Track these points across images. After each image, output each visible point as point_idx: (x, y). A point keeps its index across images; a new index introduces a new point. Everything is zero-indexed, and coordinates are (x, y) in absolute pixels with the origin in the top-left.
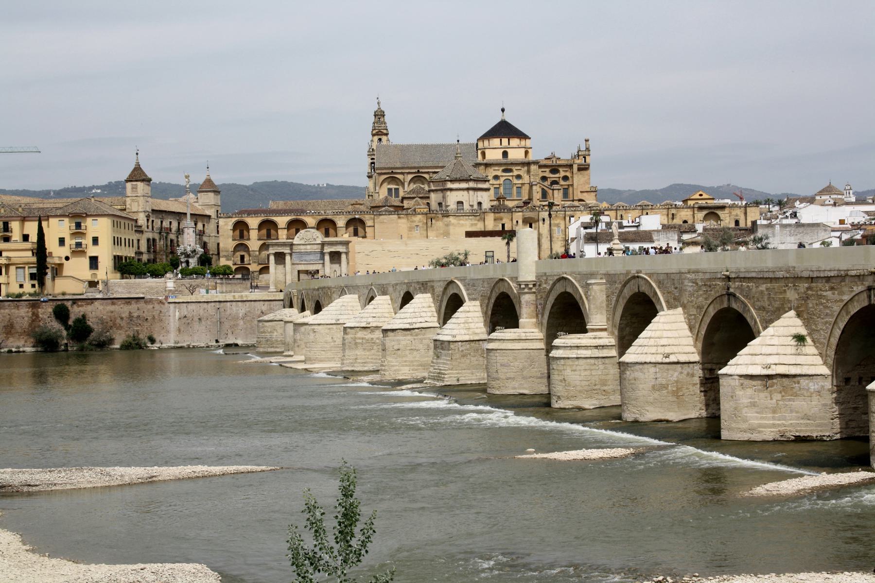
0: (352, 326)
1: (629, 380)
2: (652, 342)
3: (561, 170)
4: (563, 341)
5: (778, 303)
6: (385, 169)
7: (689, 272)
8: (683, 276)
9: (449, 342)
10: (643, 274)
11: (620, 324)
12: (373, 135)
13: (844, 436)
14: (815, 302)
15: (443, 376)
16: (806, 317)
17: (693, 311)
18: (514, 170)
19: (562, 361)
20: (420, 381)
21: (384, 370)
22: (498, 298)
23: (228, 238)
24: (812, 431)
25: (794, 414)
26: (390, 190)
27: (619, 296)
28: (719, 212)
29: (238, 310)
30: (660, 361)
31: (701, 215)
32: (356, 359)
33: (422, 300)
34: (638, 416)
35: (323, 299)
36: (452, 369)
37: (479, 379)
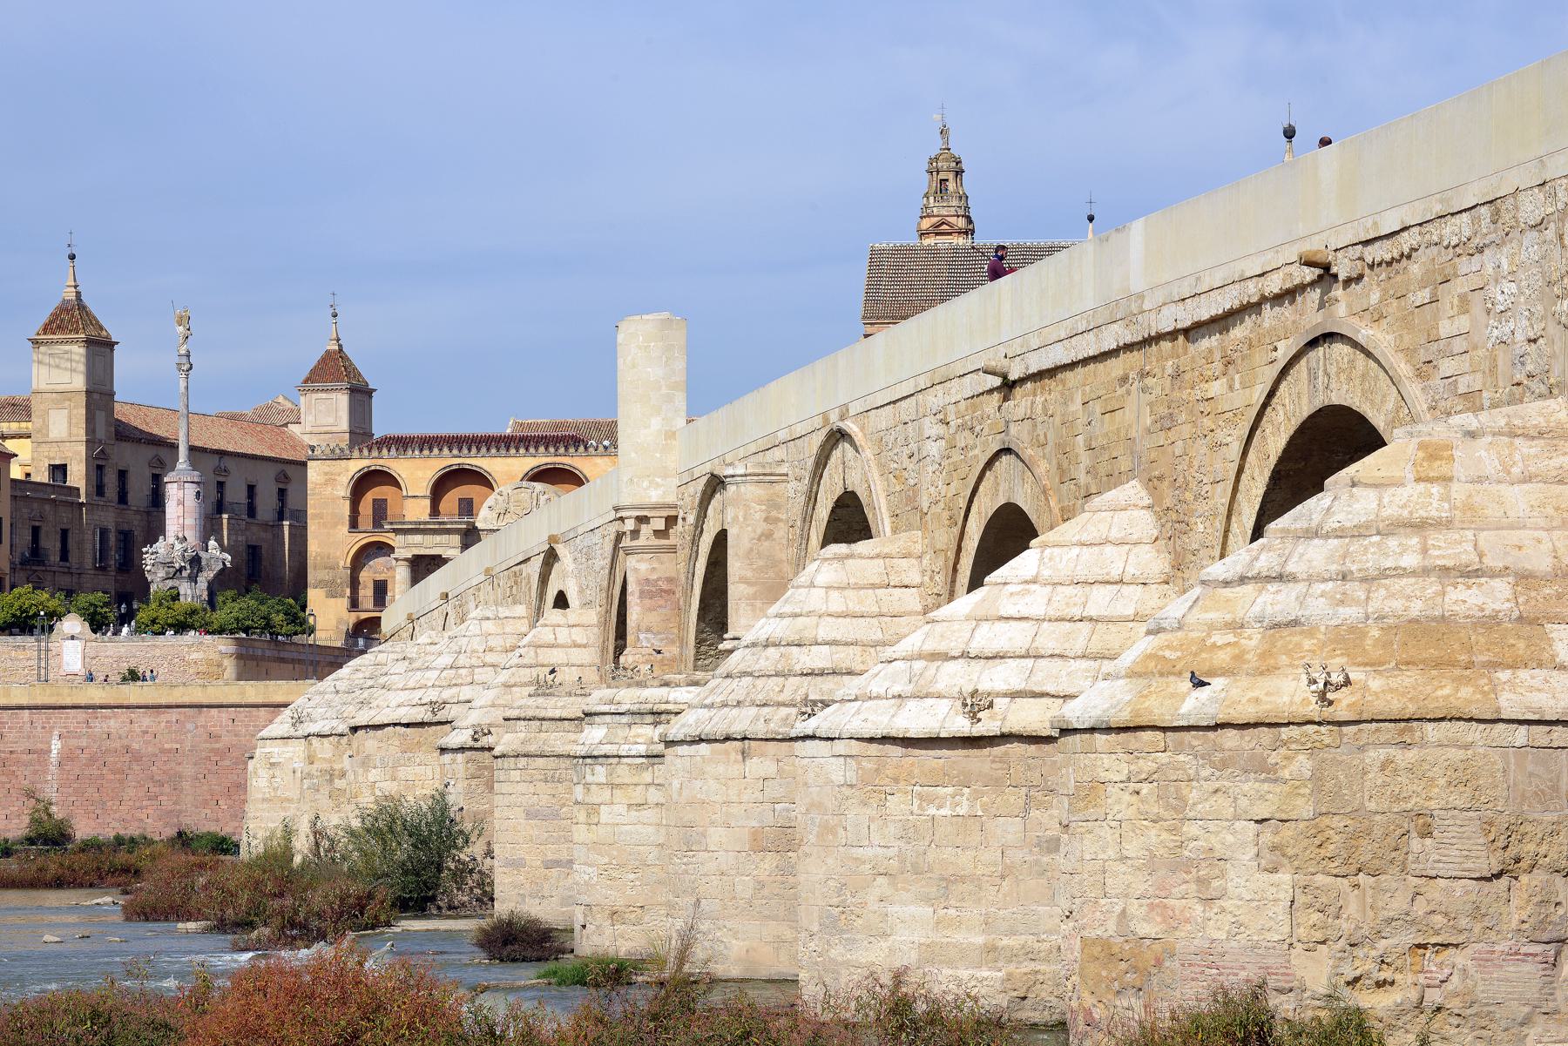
23: (335, 525)
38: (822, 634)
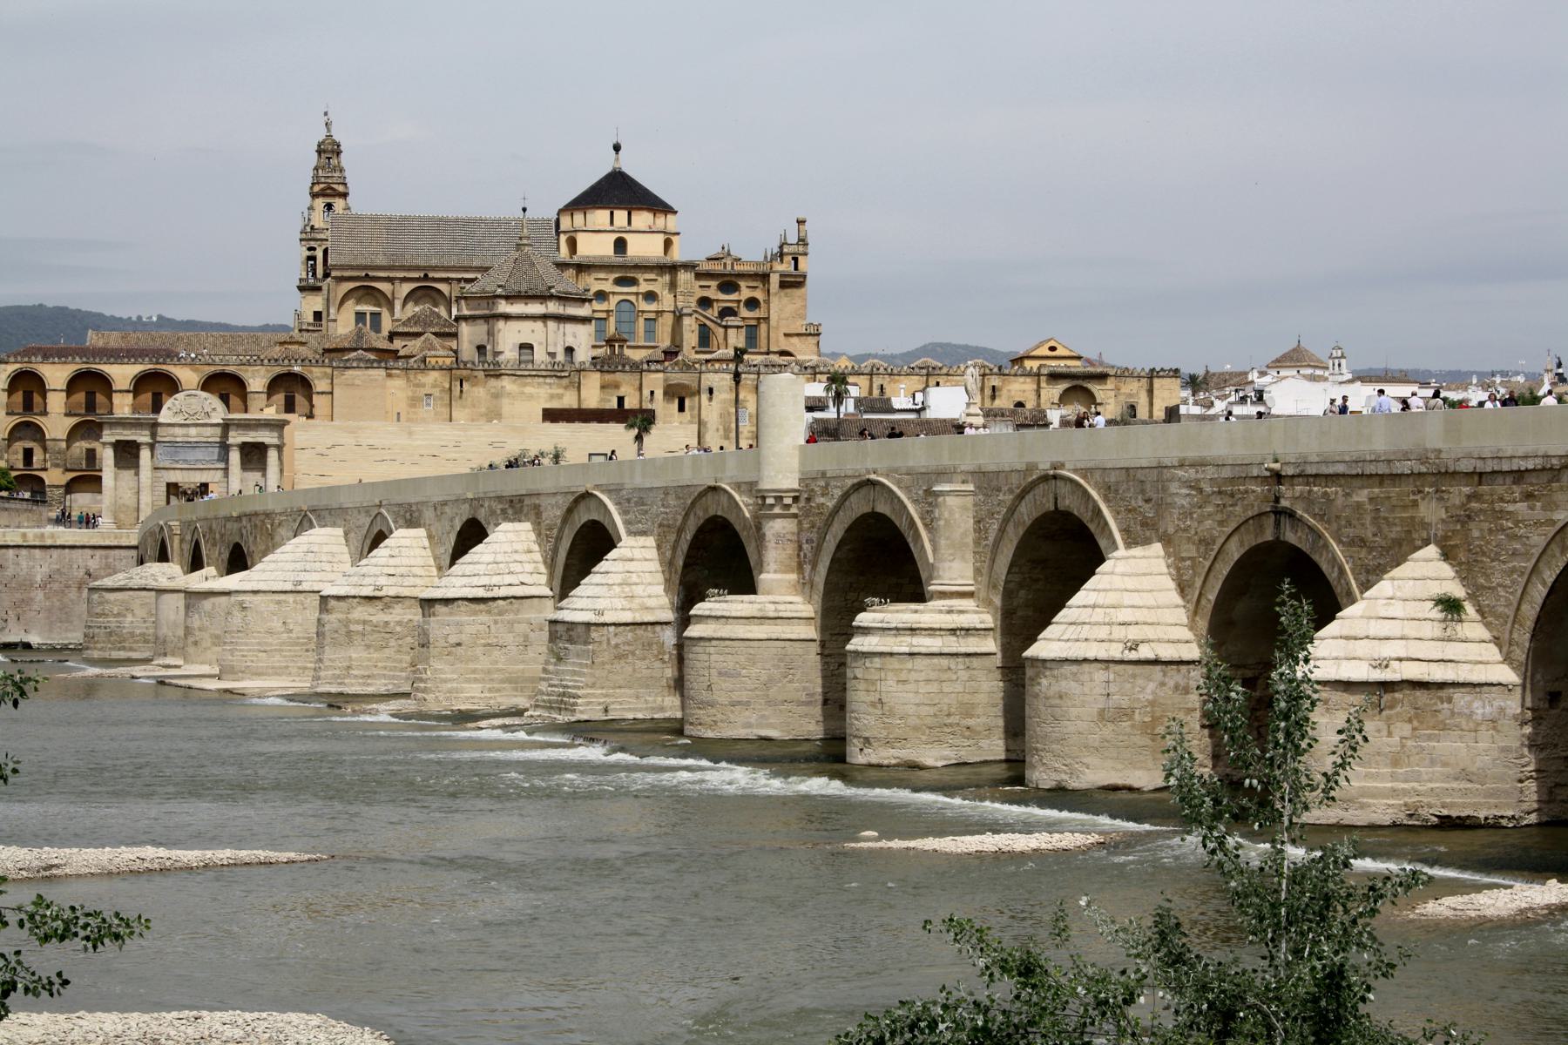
0: (342, 592)
1: (1047, 698)
2: (1098, 615)
3: (743, 284)
4: (879, 616)
5: (1399, 529)
6: (352, 268)
7: (1181, 465)
8: (1167, 474)
9: (588, 625)
10: (1069, 470)
11: (1007, 582)
12: (314, 196)
13: (1545, 819)
14: (1486, 526)
15: (572, 700)
16: (1463, 560)
17: (1190, 550)
18: (641, 281)
19: (877, 660)
20: (519, 713)
21: (425, 690)
22: (701, 531)
24: (1476, 806)
25: (1438, 769)
26: (360, 316)
27: (1006, 521)
28: (1095, 388)
29: (33, 567)
30: (1117, 655)
31: (1053, 392)
32: (349, 667)
33: (511, 536)
34: (1064, 777)
35: (251, 539)
36: (593, 686)
37: (653, 709)
38: (1127, 602)
